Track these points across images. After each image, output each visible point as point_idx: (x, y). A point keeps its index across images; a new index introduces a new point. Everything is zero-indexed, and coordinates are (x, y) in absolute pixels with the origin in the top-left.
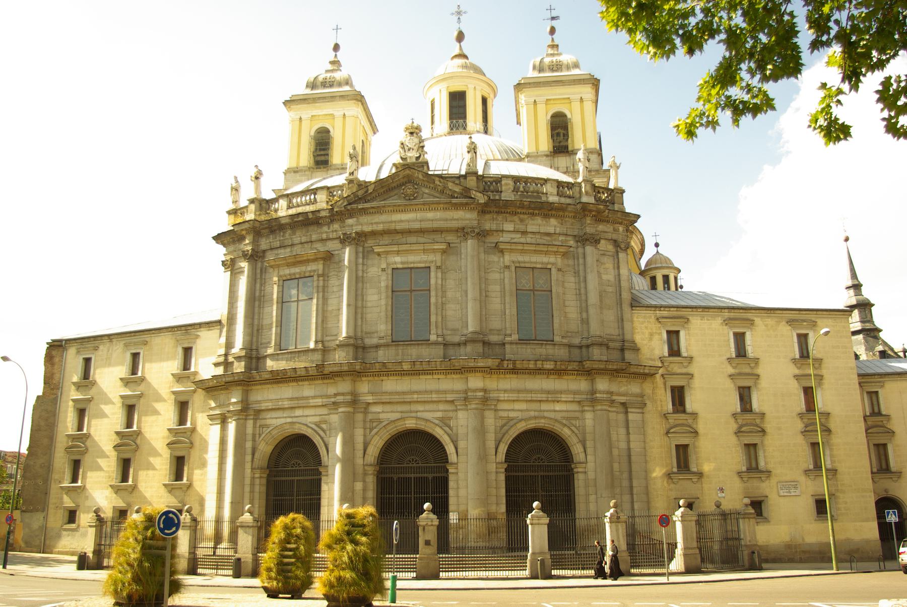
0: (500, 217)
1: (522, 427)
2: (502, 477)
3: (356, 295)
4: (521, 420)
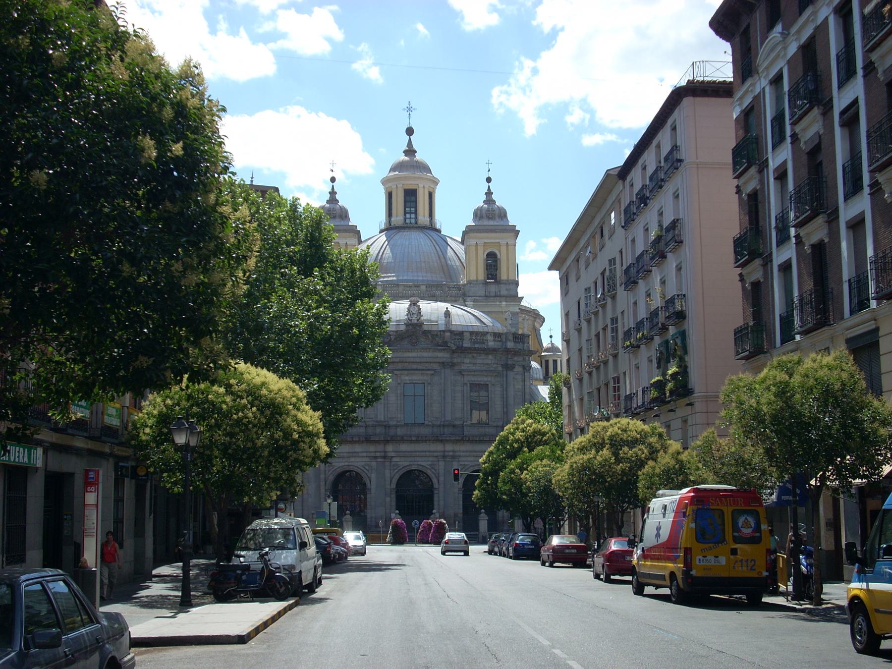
2: (461, 495)
4: (471, 466)
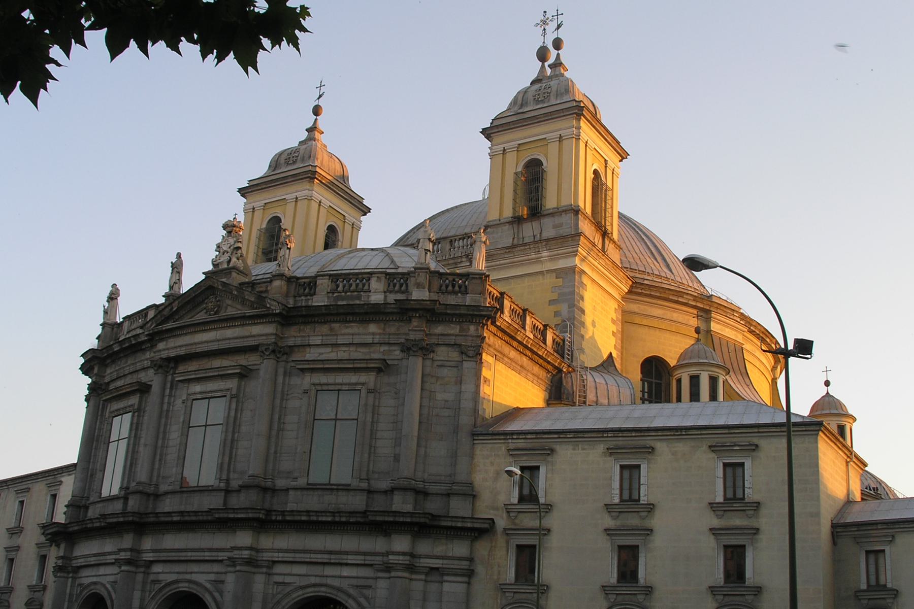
0: (308, 329)
1: (298, 595)
3: (158, 433)
